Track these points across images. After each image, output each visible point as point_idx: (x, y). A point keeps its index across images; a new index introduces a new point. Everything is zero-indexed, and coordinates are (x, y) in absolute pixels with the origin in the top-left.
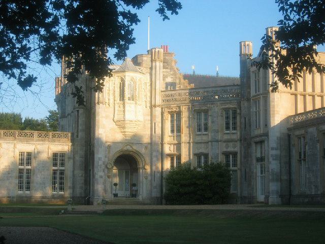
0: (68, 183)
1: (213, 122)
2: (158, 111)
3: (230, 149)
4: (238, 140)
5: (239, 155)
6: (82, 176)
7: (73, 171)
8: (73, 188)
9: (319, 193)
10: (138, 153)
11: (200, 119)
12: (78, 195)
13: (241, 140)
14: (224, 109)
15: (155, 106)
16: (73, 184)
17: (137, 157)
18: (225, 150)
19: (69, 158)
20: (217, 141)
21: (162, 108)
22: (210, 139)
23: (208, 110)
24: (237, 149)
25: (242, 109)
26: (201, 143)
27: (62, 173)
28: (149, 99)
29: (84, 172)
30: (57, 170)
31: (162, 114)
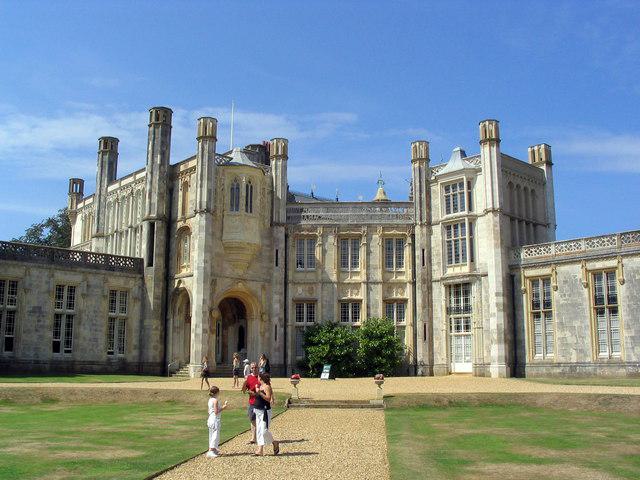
0: (133, 339)
2: (280, 233)
5: (410, 305)
7: (142, 322)
8: (142, 346)
9: (589, 360)
10: (253, 294)
12: (151, 360)
13: (414, 284)
15: (279, 224)
16: (141, 340)
19: (135, 299)
21: (286, 229)
27: (124, 322)
28: (267, 214)
31: (286, 236)
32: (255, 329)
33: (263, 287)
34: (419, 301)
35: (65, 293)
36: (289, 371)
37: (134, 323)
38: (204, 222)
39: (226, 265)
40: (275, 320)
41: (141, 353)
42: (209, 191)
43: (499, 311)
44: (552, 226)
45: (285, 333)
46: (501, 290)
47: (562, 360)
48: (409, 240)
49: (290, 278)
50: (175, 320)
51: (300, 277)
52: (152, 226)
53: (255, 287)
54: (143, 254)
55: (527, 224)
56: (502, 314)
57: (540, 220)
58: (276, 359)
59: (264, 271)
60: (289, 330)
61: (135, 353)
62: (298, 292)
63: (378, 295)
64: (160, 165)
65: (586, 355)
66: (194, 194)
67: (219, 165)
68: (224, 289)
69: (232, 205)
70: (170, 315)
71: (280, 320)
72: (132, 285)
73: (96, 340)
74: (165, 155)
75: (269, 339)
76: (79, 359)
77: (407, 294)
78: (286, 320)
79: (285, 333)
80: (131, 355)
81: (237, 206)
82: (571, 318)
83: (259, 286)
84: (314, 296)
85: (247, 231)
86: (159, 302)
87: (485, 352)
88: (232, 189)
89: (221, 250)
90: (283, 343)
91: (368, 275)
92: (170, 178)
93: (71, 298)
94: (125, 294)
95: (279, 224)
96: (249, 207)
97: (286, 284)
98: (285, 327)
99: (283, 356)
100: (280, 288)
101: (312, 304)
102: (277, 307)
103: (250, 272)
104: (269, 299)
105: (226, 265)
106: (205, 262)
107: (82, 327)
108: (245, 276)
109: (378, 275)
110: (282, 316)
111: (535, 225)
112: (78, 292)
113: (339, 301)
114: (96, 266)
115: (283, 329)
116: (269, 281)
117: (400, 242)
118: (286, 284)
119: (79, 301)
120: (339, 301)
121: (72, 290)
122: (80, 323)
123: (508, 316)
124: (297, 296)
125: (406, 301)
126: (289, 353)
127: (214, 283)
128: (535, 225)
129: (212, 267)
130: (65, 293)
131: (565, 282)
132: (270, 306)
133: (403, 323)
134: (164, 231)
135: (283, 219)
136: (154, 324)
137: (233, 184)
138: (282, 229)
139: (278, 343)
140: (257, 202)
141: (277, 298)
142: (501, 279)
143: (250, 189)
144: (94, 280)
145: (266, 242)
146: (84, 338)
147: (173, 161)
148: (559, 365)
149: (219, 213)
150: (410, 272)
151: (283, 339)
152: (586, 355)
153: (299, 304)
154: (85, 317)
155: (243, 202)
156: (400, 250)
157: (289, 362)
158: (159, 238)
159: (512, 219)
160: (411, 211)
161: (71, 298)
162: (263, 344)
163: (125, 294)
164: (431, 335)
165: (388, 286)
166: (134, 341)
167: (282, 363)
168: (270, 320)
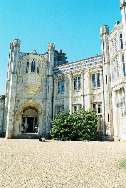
2: (50, 79)
24: (102, 100)
31: (53, 80)
33: (43, 102)
39: (24, 94)
41: (3, 128)
53: (39, 102)
62: (57, 102)
63: (88, 99)
68: (24, 103)
71: (49, 114)
83: (41, 101)
91: (84, 92)
100: (50, 101)
105: (24, 94)
108: (35, 98)
109: (87, 91)
110: (50, 113)
113: (73, 105)
116: (46, 99)
117: (99, 75)
133: (100, 114)
138: (51, 78)
140: (41, 69)
141: (49, 105)
145: (45, 83)
160: (102, 57)
162: (43, 125)
165: (92, 96)
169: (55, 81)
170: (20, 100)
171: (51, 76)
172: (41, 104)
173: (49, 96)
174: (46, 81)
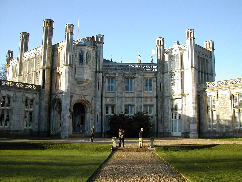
1: (137, 85)
3: (149, 103)
4: (155, 97)
6: (46, 116)
7: (39, 113)
8: (39, 124)
9: (231, 130)
10: (87, 102)
11: (127, 83)
12: (43, 130)
13: (157, 98)
14: (145, 77)
15: (99, 72)
16: (39, 121)
17: (86, 104)
18: (145, 103)
19: (37, 103)
20: (141, 97)
21: (102, 74)
22: (136, 96)
23: (134, 77)
25: (158, 78)
26: (129, 98)
28: (94, 67)
29: (47, 113)
30: (28, 111)
31: (103, 77)
32: (89, 117)
33: (92, 99)
34: (159, 105)
35: (6, 100)
36: (103, 136)
37: (36, 114)
38: (68, 70)
39: (77, 89)
40: (97, 113)
41: (39, 127)
42: (70, 57)
43: (193, 110)
44: (214, 75)
45: (102, 119)
46: (195, 101)
47: (219, 130)
48: (155, 79)
49: (104, 95)
50: (54, 113)
51: (108, 95)
52: (44, 71)
53: (89, 99)
54: (40, 84)
55: (205, 73)
56: (195, 111)
57: (210, 72)
58: (98, 130)
59: (93, 92)
60: (103, 117)
61: (37, 127)
62: (107, 101)
64: (48, 45)
65: (230, 129)
66: (63, 58)
67: (73, 46)
68: (76, 99)
69: (80, 63)
70: (52, 110)
71: (99, 113)
72: (36, 97)
73: (19, 121)
74: (50, 40)
75: (95, 121)
76: (12, 129)
77: (154, 102)
78: (102, 113)
79: (102, 119)
80: (35, 128)
81: (82, 64)
82: (223, 113)
83: (91, 98)
84: (114, 103)
85: (87, 74)
86: (47, 104)
87: (187, 127)
88: (80, 56)
89: (74, 82)
90: (100, 123)
92: (53, 51)
93: (8, 102)
94: (32, 100)
95: (99, 72)
96: (87, 63)
97: (102, 97)
98: (102, 116)
99: (100, 128)
101: (113, 106)
102: (98, 107)
103: (87, 92)
104: (95, 104)
105: (77, 89)
106: (68, 87)
107: (13, 115)
108: (85, 94)
110: (100, 111)
111: (207, 74)
112: (12, 99)
113: (125, 105)
114: (19, 88)
115: (100, 117)
116: (95, 96)
117: (151, 80)
118: (102, 97)
119: (13, 105)
120: (125, 105)
121: (9, 98)
122: (12, 113)
123: (197, 112)
124: (107, 103)
125: (152, 105)
126: (103, 128)
127: (71, 97)
128: (207, 74)
129: (71, 90)
130: (6, 100)
131: (221, 98)
132: (95, 107)
134: (49, 73)
135: (101, 70)
136: (44, 114)
137: (80, 54)
138: (101, 74)
139: (98, 123)
141: (99, 103)
142: (194, 97)
143: (88, 55)
144: (18, 94)
146: (14, 120)
147: (53, 44)
148: (218, 133)
149: (74, 65)
150: (155, 93)
151: (100, 121)
152: (230, 129)
153: (107, 106)
154: (14, 111)
155: (85, 61)
156: (151, 84)
157: (103, 131)
158: (47, 76)
159: (199, 71)
161: (8, 102)
163: (32, 100)
164: (164, 120)
166: (36, 122)
167: (100, 131)
168: (95, 113)
169: (104, 78)
170: (74, 96)
171: (101, 72)
172: (90, 101)
173: (99, 93)
174: (96, 77)
